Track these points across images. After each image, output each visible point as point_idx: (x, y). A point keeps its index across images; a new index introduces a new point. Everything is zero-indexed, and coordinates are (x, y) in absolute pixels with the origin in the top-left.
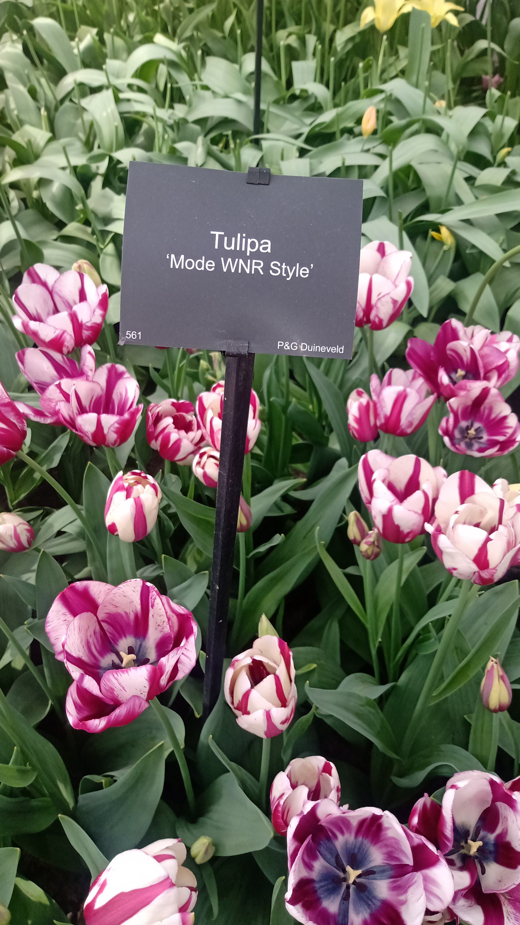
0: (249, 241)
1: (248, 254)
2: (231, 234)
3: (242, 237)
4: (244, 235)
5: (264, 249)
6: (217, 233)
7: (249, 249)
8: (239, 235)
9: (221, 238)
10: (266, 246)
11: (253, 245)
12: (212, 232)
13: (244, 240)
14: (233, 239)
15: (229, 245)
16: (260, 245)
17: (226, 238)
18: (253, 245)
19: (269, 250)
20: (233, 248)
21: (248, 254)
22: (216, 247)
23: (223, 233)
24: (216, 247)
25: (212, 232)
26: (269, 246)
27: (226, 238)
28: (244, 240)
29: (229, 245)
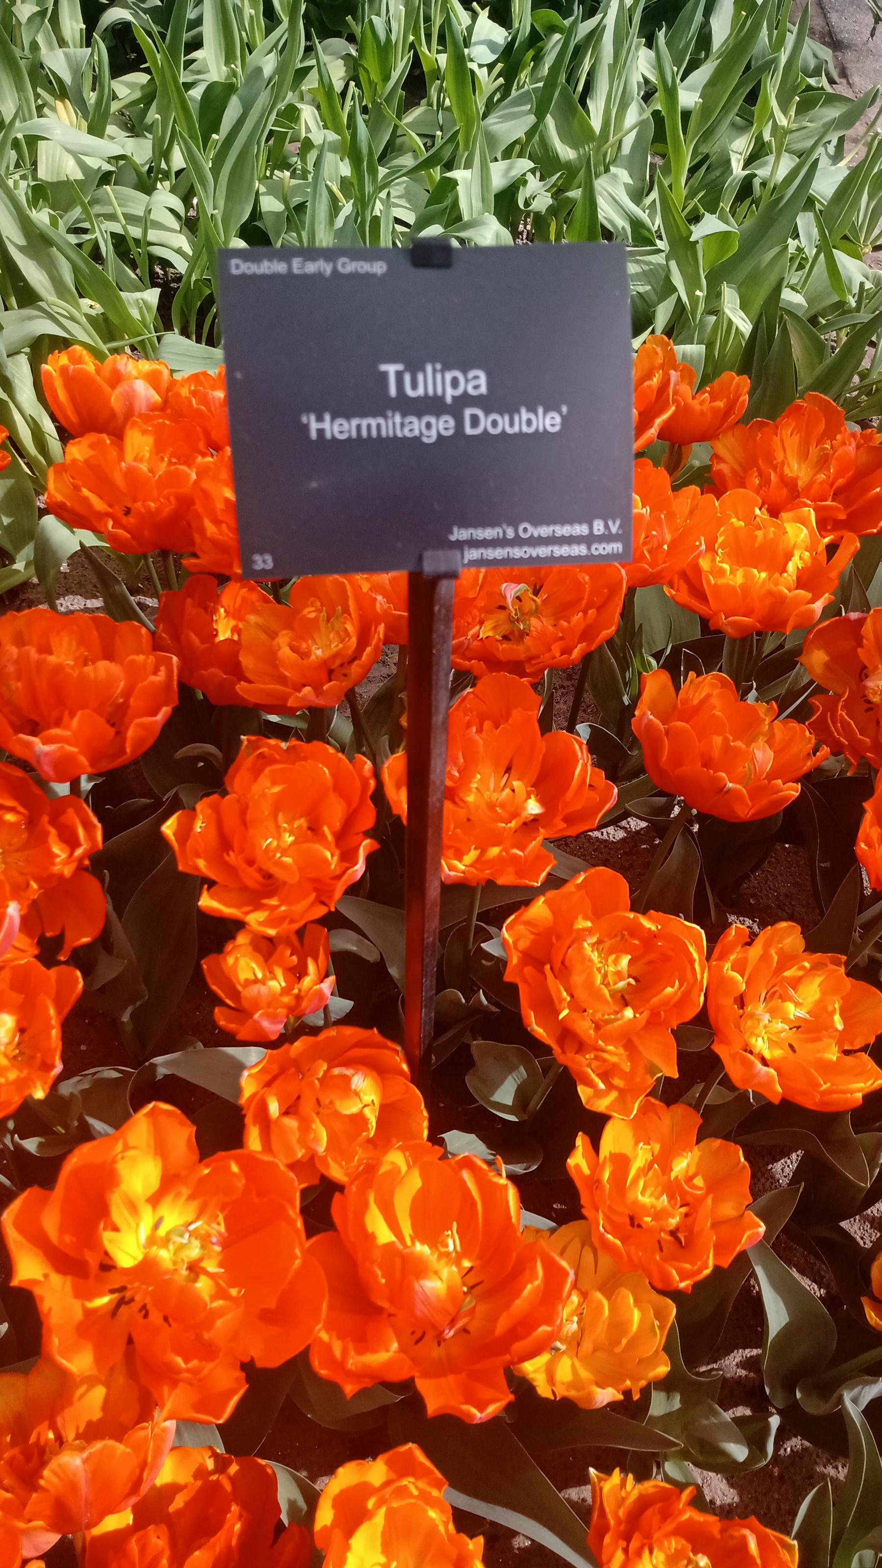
1: (449, 400)
2: (415, 367)
3: (434, 371)
4: (438, 366)
5: (476, 387)
6: (391, 369)
8: (429, 368)
9: (399, 375)
10: (478, 382)
11: (455, 383)
12: (383, 367)
13: (439, 377)
14: (420, 377)
15: (414, 386)
16: (467, 381)
17: (407, 378)
18: (455, 383)
19: (483, 390)
20: (420, 391)
21: (449, 400)
22: (393, 391)
23: (400, 367)
24: (393, 391)
25: (383, 367)
27: (407, 378)
28: (439, 377)
29: (414, 386)
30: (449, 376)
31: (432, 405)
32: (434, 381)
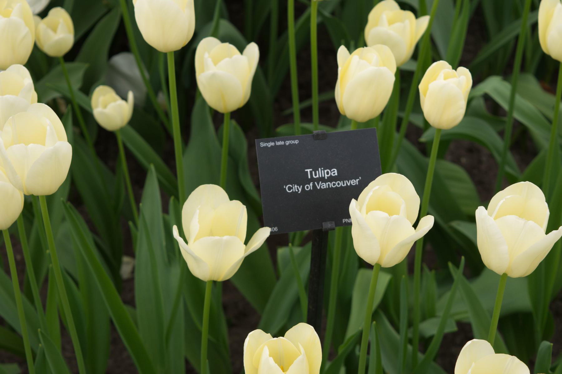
0: (326, 171)
2: (315, 170)
3: (321, 170)
5: (334, 174)
6: (309, 170)
7: (326, 175)
8: (320, 169)
10: (335, 172)
11: (328, 173)
15: (316, 175)
17: (313, 172)
18: (328, 173)
19: (336, 174)
20: (318, 176)
22: (309, 177)
24: (309, 177)
26: (336, 172)
27: (313, 172)
29: (316, 175)
30: (326, 171)
31: (322, 180)
32: (322, 173)
